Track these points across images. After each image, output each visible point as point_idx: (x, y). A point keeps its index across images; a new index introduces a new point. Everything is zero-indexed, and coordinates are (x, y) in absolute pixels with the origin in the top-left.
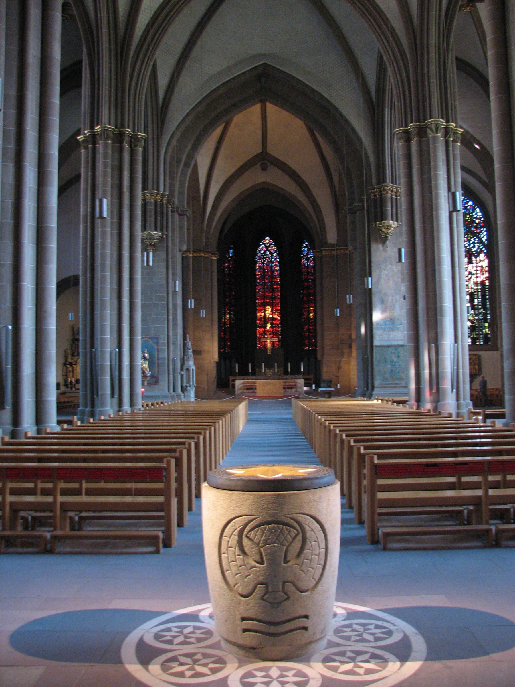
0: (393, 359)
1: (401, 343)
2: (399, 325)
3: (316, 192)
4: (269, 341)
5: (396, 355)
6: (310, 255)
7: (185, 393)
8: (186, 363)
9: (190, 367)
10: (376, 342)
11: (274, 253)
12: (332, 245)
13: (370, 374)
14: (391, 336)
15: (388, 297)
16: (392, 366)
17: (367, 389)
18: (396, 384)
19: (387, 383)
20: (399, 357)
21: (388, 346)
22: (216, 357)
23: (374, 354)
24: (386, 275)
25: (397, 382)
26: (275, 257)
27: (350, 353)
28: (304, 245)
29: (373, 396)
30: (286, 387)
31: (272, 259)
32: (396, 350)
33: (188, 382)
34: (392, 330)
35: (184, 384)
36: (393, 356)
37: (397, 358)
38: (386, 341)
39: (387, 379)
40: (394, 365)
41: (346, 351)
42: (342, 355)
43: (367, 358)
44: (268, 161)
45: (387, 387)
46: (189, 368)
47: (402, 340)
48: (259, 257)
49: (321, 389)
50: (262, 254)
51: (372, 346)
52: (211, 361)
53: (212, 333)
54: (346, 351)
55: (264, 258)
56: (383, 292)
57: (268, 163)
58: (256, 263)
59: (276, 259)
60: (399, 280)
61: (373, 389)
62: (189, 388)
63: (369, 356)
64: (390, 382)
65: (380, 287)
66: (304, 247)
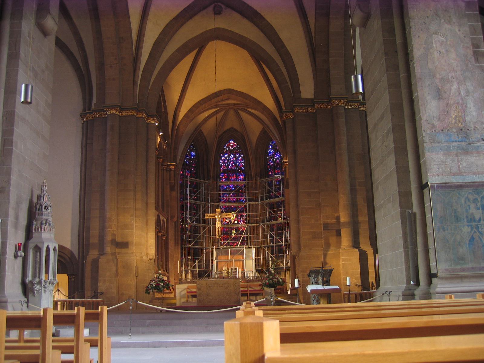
0: (472, 214)
2: (478, 142)
3: (284, 35)
4: (218, 217)
5: (479, 205)
6: (277, 156)
7: (30, 296)
8: (35, 235)
9: (43, 243)
11: (239, 157)
12: (307, 100)
13: (420, 249)
14: (465, 164)
15: (449, 85)
16: (472, 228)
17: (417, 284)
19: (464, 266)
21: (460, 186)
22: (152, 252)
23: (427, 205)
24: (442, 43)
26: (240, 160)
27: (339, 243)
28: (271, 147)
30: (248, 292)
31: (237, 162)
32: (478, 194)
33: (37, 274)
34: (466, 152)
35: (29, 278)
37: (481, 211)
38: (454, 175)
39: (461, 259)
40: (477, 227)
41: (333, 240)
42: (328, 245)
43: (415, 214)
44: (222, 3)
45: (466, 277)
46: (40, 245)
48: (223, 160)
49: (309, 288)
50: (226, 158)
51: (422, 186)
52: (142, 257)
53: (147, 221)
54: (333, 240)
55: (228, 161)
56: (438, 76)
57: (223, 6)
58: (221, 167)
59: (241, 162)
60: (470, 52)
61: (430, 283)
62: (37, 287)
63: (416, 209)
64: (470, 265)
65: (430, 66)
66: (270, 149)
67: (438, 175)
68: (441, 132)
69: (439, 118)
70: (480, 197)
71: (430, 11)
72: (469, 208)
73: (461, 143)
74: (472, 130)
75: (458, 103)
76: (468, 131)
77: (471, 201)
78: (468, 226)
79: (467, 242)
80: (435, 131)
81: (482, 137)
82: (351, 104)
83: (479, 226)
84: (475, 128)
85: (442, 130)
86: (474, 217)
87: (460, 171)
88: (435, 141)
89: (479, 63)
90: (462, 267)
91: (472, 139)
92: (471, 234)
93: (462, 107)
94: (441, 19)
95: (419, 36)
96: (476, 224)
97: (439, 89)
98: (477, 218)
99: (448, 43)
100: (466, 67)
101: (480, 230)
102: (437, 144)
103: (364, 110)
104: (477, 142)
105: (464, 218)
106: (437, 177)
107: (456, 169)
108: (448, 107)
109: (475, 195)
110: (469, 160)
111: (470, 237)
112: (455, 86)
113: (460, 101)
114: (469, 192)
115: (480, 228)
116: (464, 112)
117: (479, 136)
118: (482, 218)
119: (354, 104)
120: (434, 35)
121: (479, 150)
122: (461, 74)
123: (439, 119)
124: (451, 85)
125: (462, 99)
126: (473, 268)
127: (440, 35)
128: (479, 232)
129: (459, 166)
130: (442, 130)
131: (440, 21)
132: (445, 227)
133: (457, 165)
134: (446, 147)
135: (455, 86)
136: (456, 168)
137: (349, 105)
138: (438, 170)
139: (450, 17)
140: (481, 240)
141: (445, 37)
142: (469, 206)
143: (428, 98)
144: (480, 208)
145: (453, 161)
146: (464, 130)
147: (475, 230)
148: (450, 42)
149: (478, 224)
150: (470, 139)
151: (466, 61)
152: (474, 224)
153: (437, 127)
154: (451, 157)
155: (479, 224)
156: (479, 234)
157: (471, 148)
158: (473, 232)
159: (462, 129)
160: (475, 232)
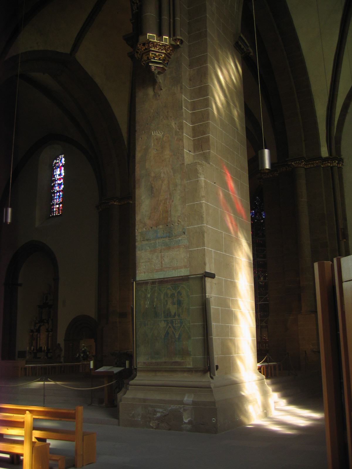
0: (169, 309)
1: (184, 272)
5: (175, 300)
10: (141, 275)
14: (166, 260)
18: (176, 363)
19: (159, 361)
20: (180, 303)
25: (178, 359)
29: (130, 387)
34: (169, 248)
36: (170, 302)
37: (176, 306)
38: (157, 271)
40: (172, 322)
47: (185, 267)
56: (153, 175)
64: (163, 360)
67: (145, 273)
68: (150, 229)
69: (150, 216)
70: (177, 291)
71: (152, 111)
72: (167, 303)
73: (165, 239)
74: (177, 224)
75: (166, 199)
76: (172, 226)
77: (169, 296)
78: (164, 321)
79: (163, 337)
80: (146, 229)
81: (184, 231)
82: (312, 162)
83: (173, 321)
84: (178, 222)
85: (152, 228)
86: (170, 312)
87: (162, 266)
88: (145, 240)
89: (202, 151)
90: (157, 361)
91: (175, 233)
92: (167, 330)
93: (169, 202)
94: (160, 116)
95: (141, 138)
96: (171, 319)
97: (152, 187)
98: (173, 314)
99: (164, 139)
100: (177, 160)
101: (174, 325)
102: (146, 242)
103: (329, 166)
104: (179, 236)
105: (162, 314)
106: (143, 274)
107: (159, 265)
108: (158, 204)
109: (173, 290)
110: (170, 255)
111: (166, 331)
112: (166, 182)
113: (169, 196)
114: (168, 287)
115: (174, 322)
116: (171, 207)
117: (181, 230)
118: (176, 313)
119: (315, 162)
120: (153, 134)
121: (180, 245)
122: (172, 169)
123: (149, 218)
124: (162, 182)
125: (170, 194)
126: (165, 362)
127: (159, 133)
128: (173, 327)
129: (161, 262)
130: (152, 228)
131: (160, 118)
132: (146, 322)
133: (161, 261)
134: (153, 244)
135: (166, 182)
136: (159, 264)
137: (309, 164)
138: (145, 267)
139: (168, 112)
140: (174, 334)
141: (162, 134)
142: (167, 301)
143: (143, 198)
144: (176, 303)
145: (157, 257)
146: (168, 226)
147: (170, 325)
148: (166, 138)
149: (173, 319)
150: (174, 234)
151: (178, 154)
152: (169, 319)
153: (148, 225)
154: (156, 254)
155: (174, 320)
156: (173, 330)
157: (174, 243)
158: (168, 327)
159: (168, 224)
160: (170, 327)
